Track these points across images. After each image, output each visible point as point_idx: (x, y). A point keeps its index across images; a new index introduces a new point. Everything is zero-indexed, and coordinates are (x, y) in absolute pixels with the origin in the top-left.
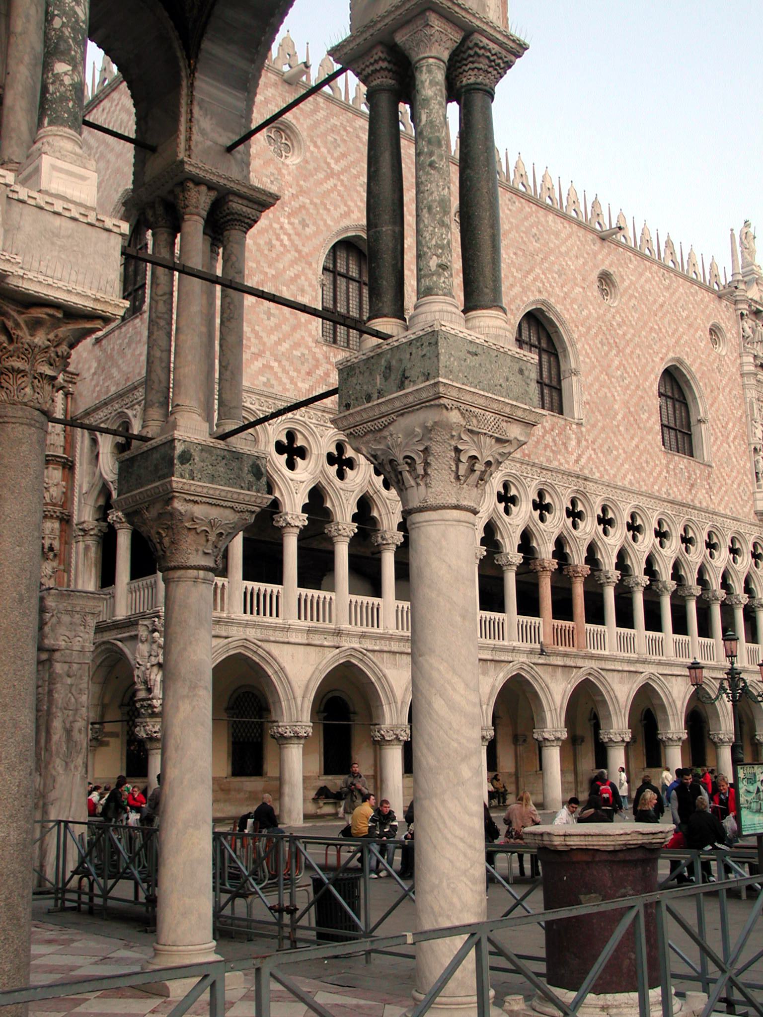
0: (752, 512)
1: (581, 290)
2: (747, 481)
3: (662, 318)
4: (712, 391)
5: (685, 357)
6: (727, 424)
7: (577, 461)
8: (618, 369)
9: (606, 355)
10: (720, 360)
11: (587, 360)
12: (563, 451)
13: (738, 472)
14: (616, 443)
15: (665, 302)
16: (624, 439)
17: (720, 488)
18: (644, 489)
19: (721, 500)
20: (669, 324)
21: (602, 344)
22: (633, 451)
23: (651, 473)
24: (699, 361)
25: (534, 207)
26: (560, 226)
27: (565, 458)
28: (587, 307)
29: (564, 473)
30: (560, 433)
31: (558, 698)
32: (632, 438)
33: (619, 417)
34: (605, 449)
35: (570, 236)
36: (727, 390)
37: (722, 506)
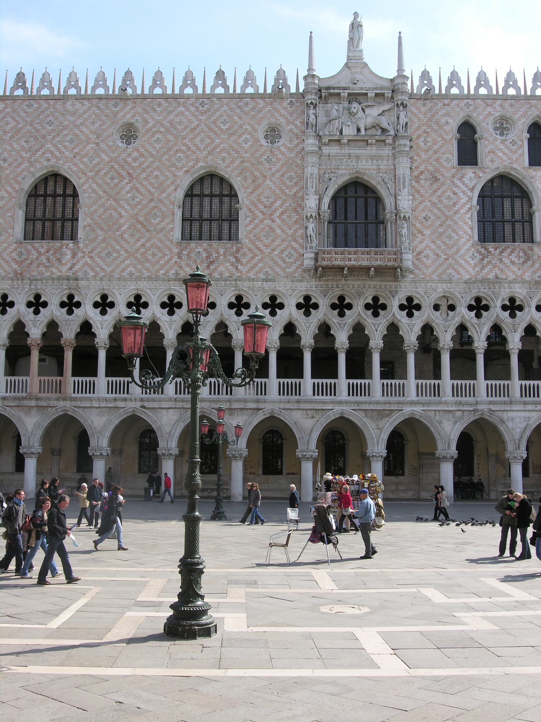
0: (300, 270)
1: (95, 146)
2: (297, 246)
3: (191, 140)
4: (254, 181)
5: (222, 162)
6: (273, 203)
7: (70, 269)
8: (129, 192)
9: (116, 185)
10: (271, 151)
11: (93, 195)
12: (56, 264)
13: (283, 241)
14: (118, 248)
15: (199, 125)
16: (128, 243)
17: (252, 258)
18: (146, 274)
19: (252, 268)
20: (202, 141)
21: (112, 178)
22: (137, 250)
23: (157, 262)
24: (239, 160)
25: (52, 102)
26: (78, 105)
27: (57, 269)
28: (98, 156)
29: (53, 279)
30: (55, 253)
31: (30, 427)
32: (138, 240)
33: (124, 228)
34: (103, 255)
35: (89, 109)
36: (278, 175)
37: (254, 272)
